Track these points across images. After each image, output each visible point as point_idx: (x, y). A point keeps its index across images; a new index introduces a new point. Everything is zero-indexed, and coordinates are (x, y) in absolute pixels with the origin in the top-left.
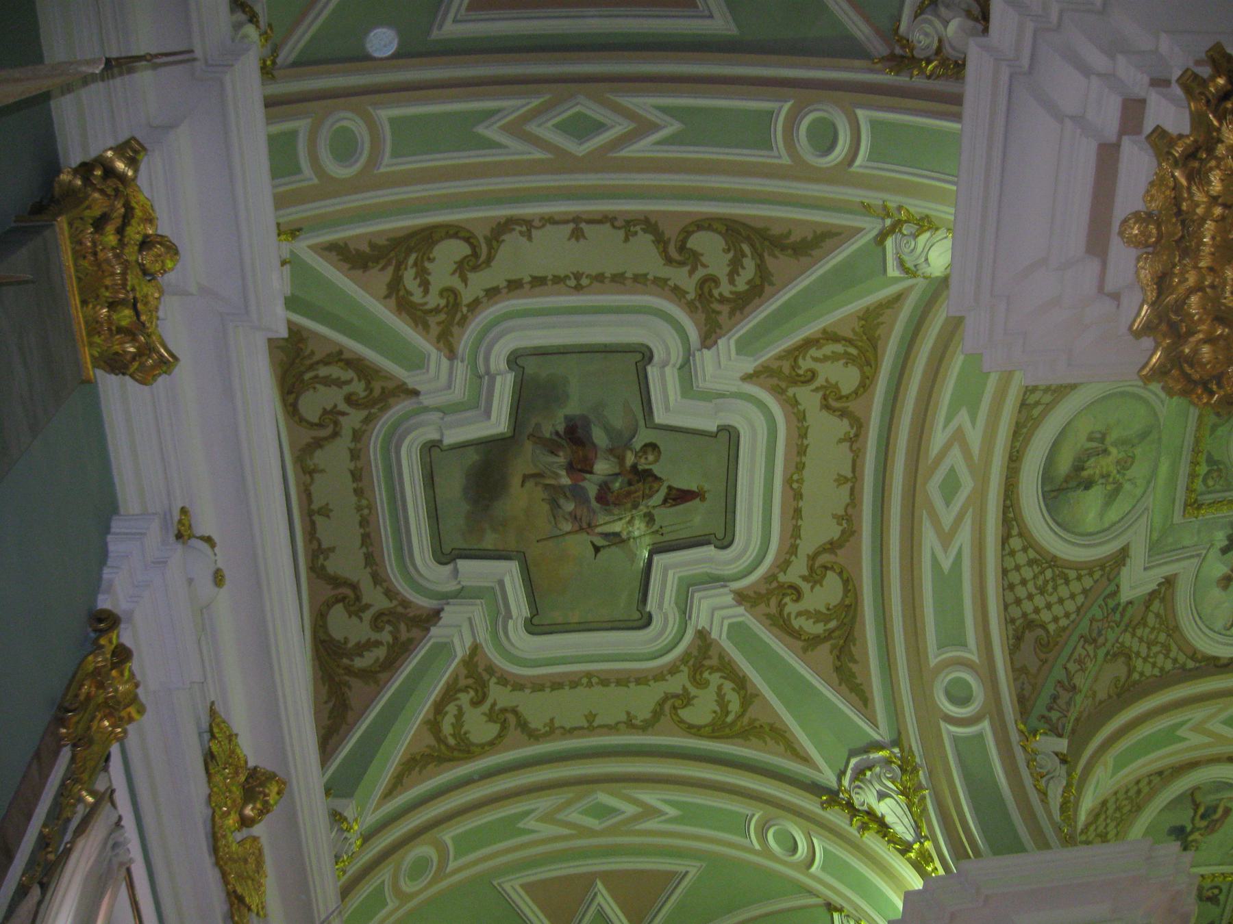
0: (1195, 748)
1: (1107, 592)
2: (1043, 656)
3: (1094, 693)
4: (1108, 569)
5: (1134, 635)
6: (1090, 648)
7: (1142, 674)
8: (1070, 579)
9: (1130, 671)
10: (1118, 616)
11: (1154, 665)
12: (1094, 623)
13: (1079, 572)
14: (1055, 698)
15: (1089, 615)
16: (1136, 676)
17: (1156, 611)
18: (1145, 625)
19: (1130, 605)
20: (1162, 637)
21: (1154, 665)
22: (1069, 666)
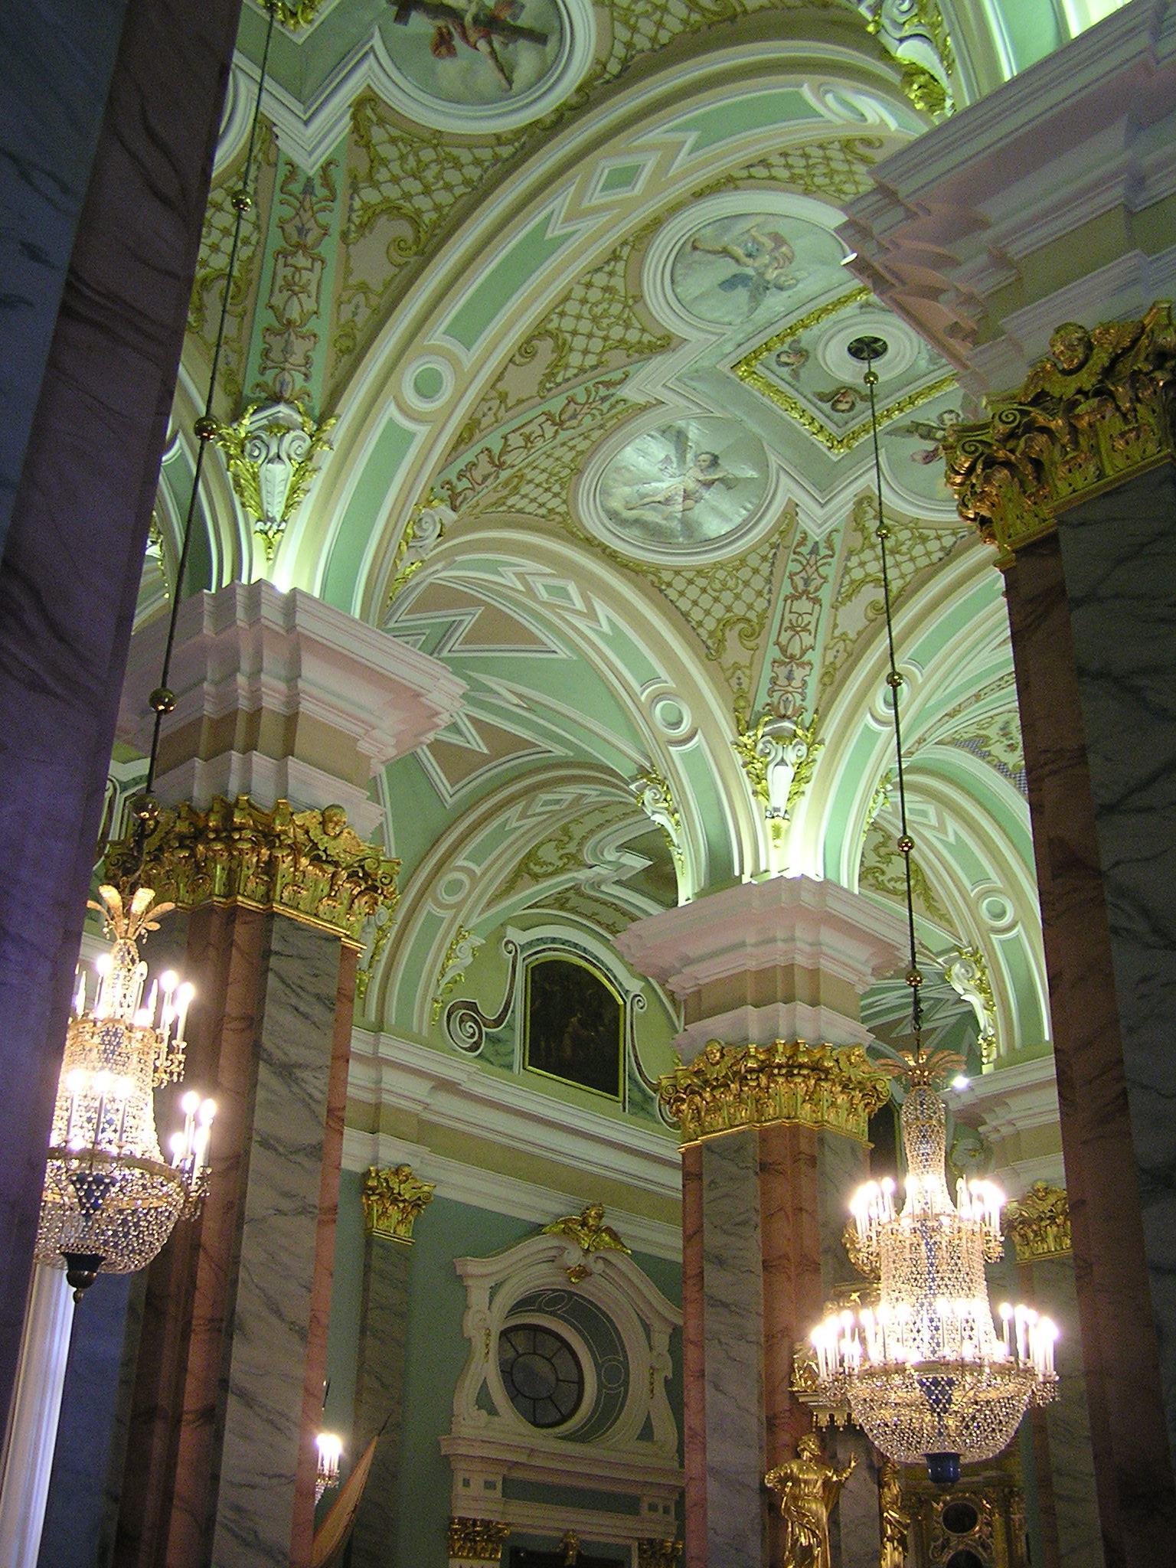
0: (593, 239)
1: (280, 178)
2: (240, 309)
3: (364, 288)
4: (260, 157)
5: (376, 185)
6: (301, 261)
7: (438, 208)
8: (220, 201)
9: (414, 220)
10: (321, 192)
11: (448, 187)
12: (286, 226)
13: (225, 186)
14: (266, 353)
15: (274, 221)
16: (428, 217)
17: (386, 137)
18: (384, 162)
19: (332, 167)
20: (428, 155)
21: (448, 187)
22: (274, 302)
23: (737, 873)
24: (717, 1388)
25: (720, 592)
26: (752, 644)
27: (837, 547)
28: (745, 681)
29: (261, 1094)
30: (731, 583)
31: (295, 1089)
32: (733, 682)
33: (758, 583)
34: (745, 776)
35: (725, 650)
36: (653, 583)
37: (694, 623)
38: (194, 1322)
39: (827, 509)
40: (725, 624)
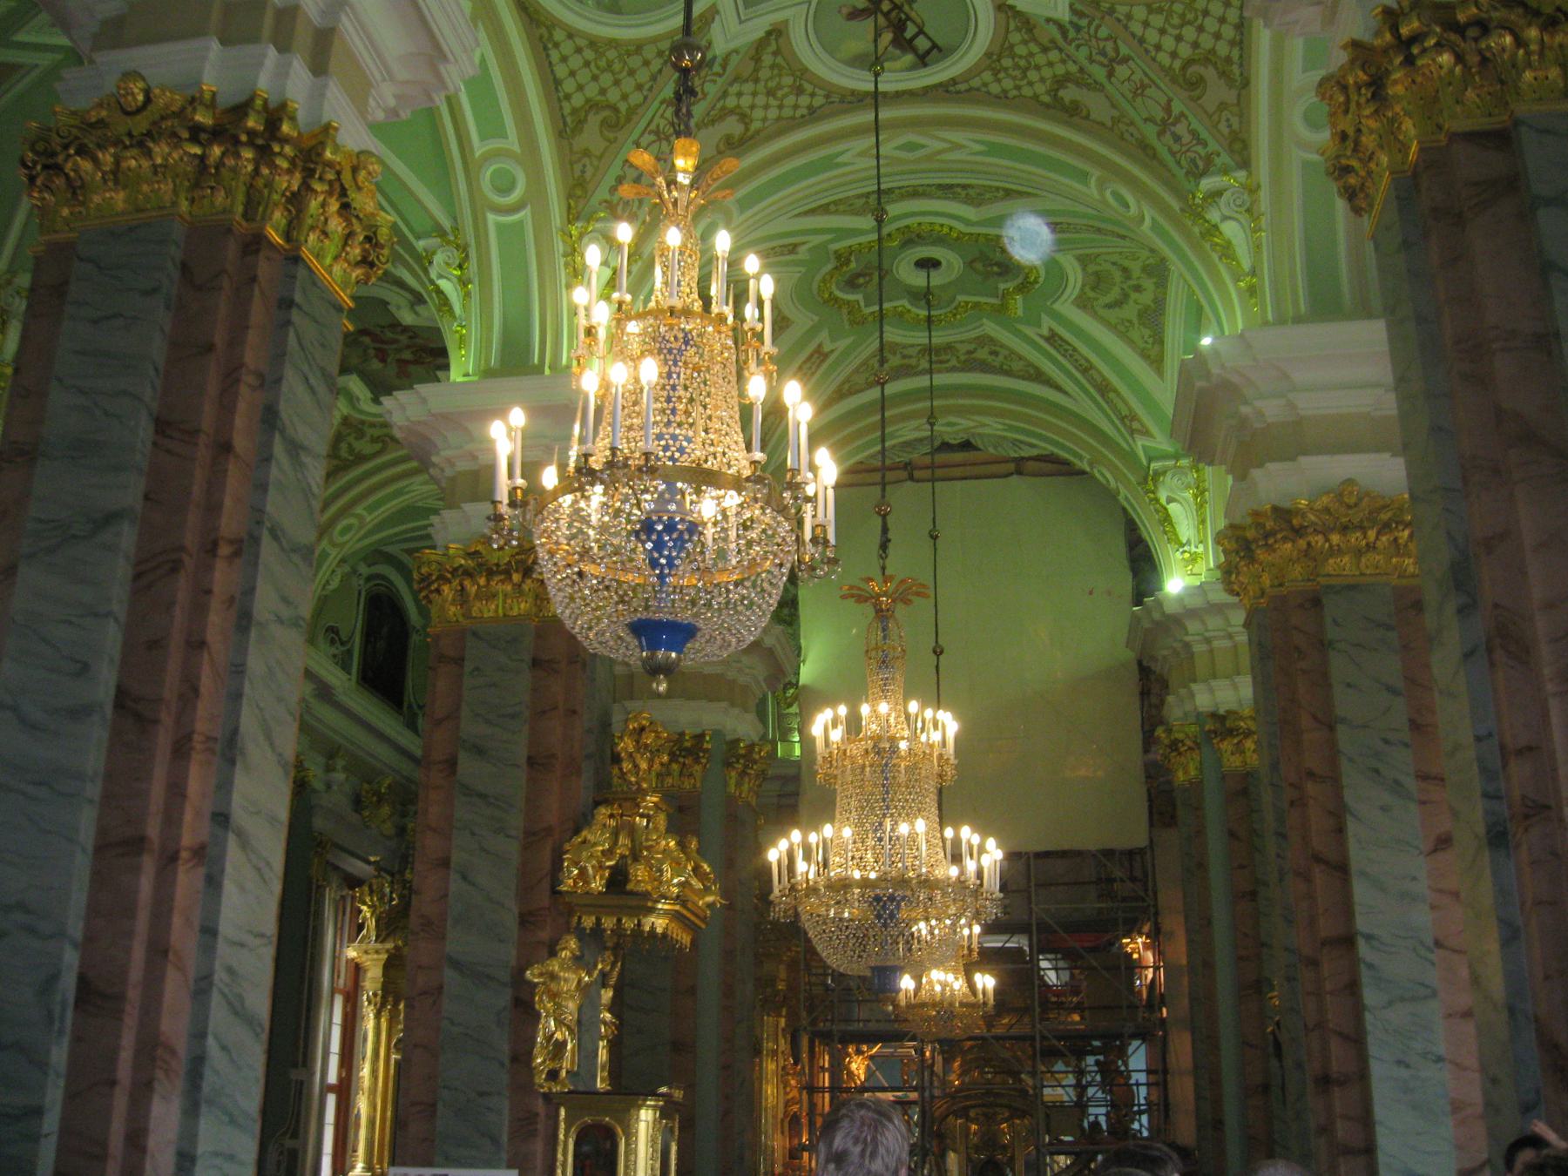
23: (536, 361)
24: (464, 878)
25: (603, 71)
26: (611, 136)
27: (730, 69)
28: (589, 171)
29: (274, 472)
30: (617, 66)
31: (300, 476)
32: (577, 167)
33: (643, 76)
34: (562, 267)
35: (581, 131)
36: (541, 37)
37: (561, 95)
38: (196, 737)
39: (743, 26)
40: (592, 106)
